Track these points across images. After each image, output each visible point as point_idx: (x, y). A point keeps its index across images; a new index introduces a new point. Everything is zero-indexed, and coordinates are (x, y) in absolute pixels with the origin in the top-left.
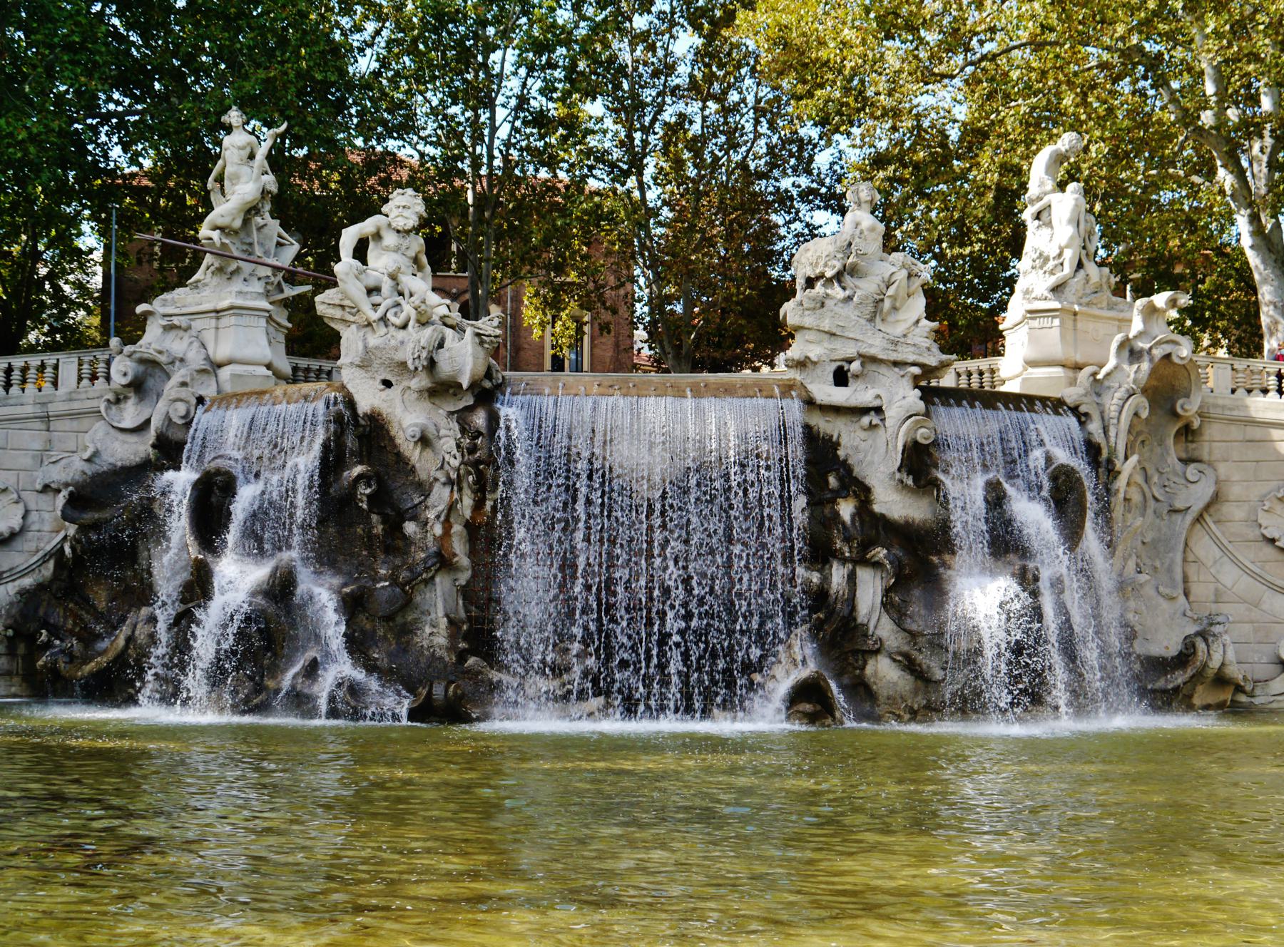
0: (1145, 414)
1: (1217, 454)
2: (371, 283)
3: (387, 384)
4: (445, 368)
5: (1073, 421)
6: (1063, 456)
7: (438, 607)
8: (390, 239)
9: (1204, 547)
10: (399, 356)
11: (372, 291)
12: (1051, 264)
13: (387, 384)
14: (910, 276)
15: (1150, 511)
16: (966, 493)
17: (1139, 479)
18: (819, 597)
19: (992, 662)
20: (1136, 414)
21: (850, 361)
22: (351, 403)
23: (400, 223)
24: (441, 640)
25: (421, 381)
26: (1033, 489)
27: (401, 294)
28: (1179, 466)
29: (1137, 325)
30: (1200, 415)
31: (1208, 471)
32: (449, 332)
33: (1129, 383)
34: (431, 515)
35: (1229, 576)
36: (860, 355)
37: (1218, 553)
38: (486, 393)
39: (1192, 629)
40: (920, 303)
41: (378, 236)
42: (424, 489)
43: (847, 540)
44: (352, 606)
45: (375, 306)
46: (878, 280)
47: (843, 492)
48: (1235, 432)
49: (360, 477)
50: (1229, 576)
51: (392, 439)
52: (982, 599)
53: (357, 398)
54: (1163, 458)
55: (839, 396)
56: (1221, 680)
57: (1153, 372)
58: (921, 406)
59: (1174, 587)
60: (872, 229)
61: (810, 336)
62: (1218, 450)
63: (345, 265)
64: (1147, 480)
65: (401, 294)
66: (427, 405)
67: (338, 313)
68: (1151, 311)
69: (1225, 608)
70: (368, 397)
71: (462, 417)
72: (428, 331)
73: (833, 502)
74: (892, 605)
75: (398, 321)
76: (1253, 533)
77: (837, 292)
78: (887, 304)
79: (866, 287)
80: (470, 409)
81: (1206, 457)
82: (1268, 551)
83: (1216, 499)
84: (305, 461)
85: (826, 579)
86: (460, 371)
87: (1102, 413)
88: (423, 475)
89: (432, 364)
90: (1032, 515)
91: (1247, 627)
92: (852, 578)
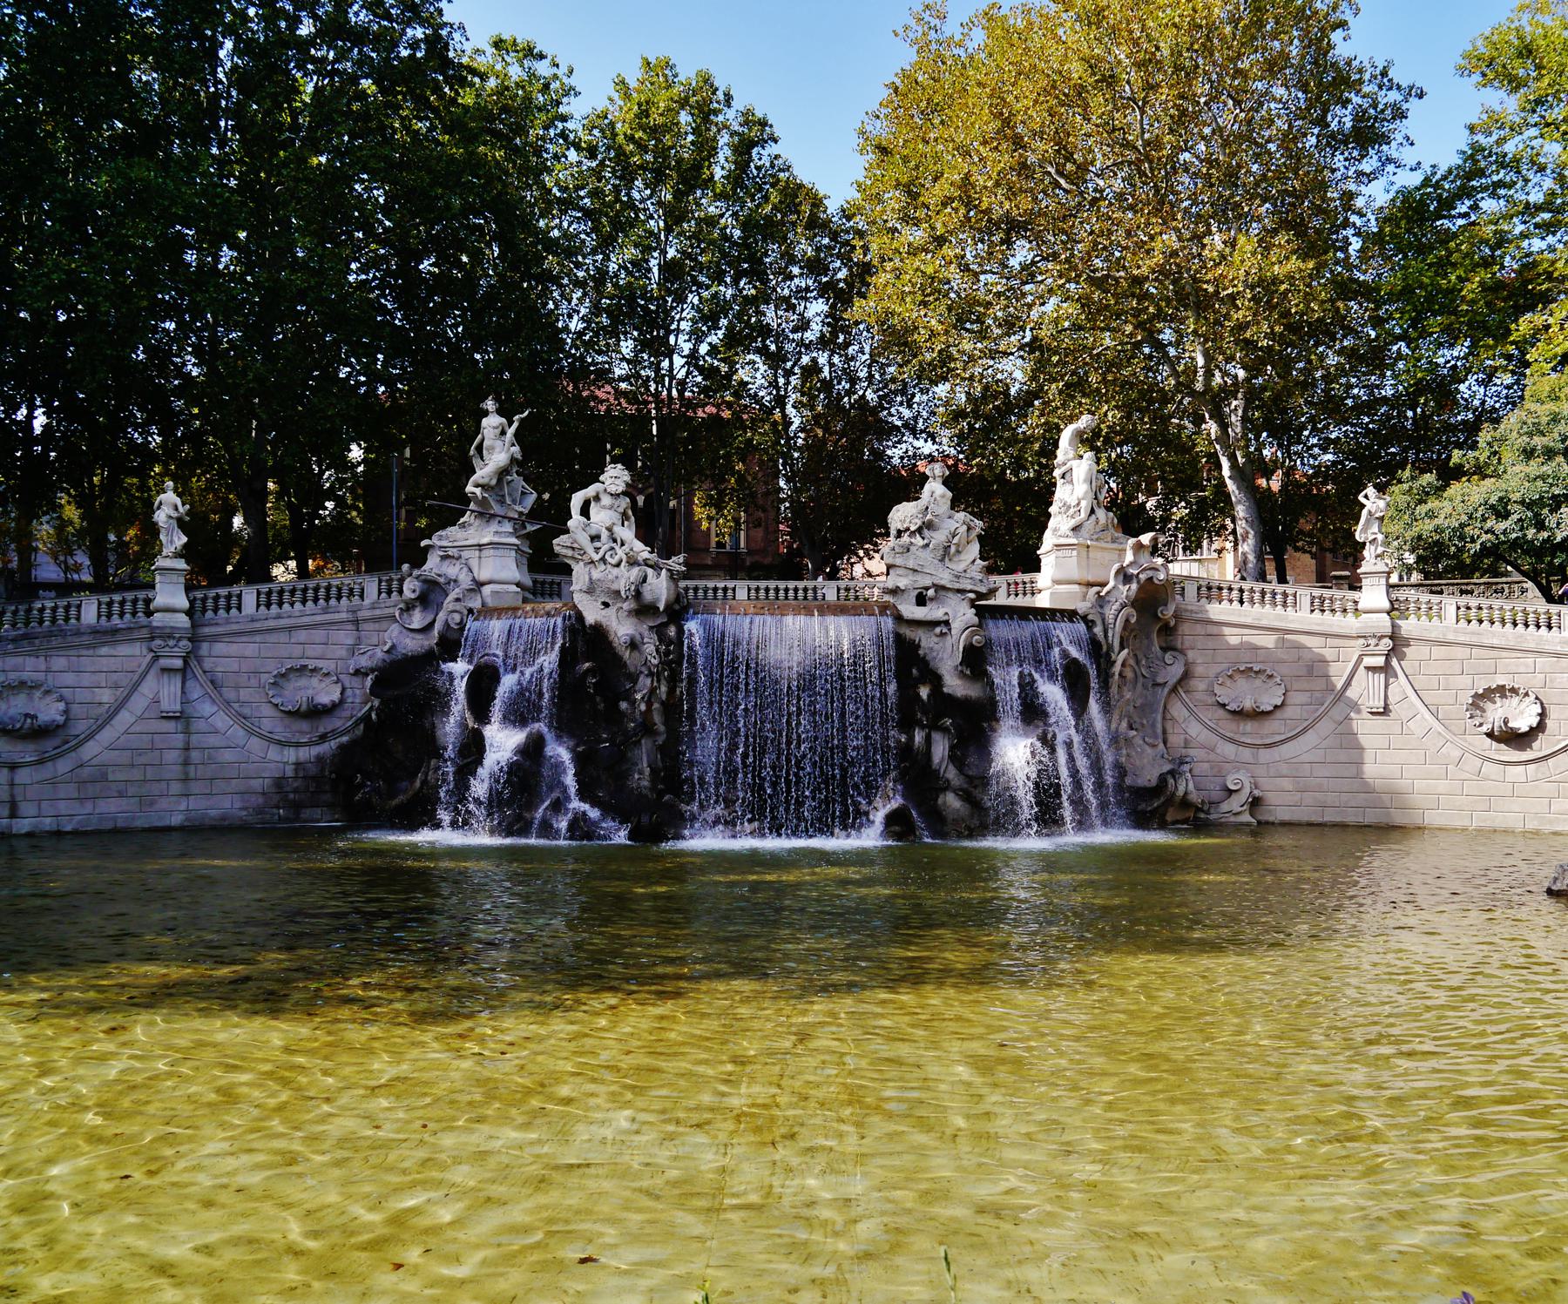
0: (1133, 620)
1: (1187, 644)
2: (593, 533)
3: (606, 605)
4: (648, 596)
5: (1082, 627)
6: (1074, 652)
7: (643, 759)
8: (606, 500)
9: (1177, 710)
10: (615, 587)
11: (595, 538)
12: (1072, 511)
13: (606, 605)
14: (969, 529)
15: (1139, 685)
16: (1006, 679)
17: (1132, 662)
18: (906, 750)
19: (1025, 797)
20: (1127, 621)
21: (927, 589)
22: (580, 617)
23: (613, 489)
24: (646, 783)
25: (629, 605)
26: (1052, 677)
27: (615, 541)
28: (1160, 653)
29: (1129, 557)
30: (1175, 616)
31: (1180, 657)
32: (650, 571)
33: (1123, 598)
34: (638, 696)
35: (1194, 729)
36: (934, 585)
37: (1187, 714)
38: (678, 611)
39: (1167, 767)
40: (974, 549)
41: (597, 498)
42: (634, 679)
43: (925, 713)
44: (580, 760)
45: (597, 550)
46: (946, 532)
47: (922, 680)
48: (1199, 629)
49: (588, 670)
50: (1194, 729)
51: (610, 643)
52: (1015, 754)
53: (585, 614)
54: (1149, 647)
55: (920, 613)
56: (1185, 803)
57: (1140, 589)
58: (976, 620)
59: (1156, 737)
60: (943, 496)
61: (900, 571)
62: (1188, 641)
63: (576, 520)
64: (1138, 662)
65: (615, 541)
66: (634, 620)
67: (570, 553)
68: (1139, 547)
69: (1192, 752)
70: (592, 613)
71: (660, 630)
72: (635, 570)
73: (916, 687)
74: (955, 757)
75: (614, 561)
76: (1211, 700)
77: (918, 541)
78: (953, 549)
79: (939, 537)
80: (665, 625)
81: (1179, 646)
82: (1221, 712)
83: (1186, 676)
84: (549, 660)
85: (911, 738)
86: (658, 600)
87: (1103, 620)
88: (632, 669)
89: (638, 595)
90: (1053, 694)
91: (1206, 765)
92: (928, 740)
